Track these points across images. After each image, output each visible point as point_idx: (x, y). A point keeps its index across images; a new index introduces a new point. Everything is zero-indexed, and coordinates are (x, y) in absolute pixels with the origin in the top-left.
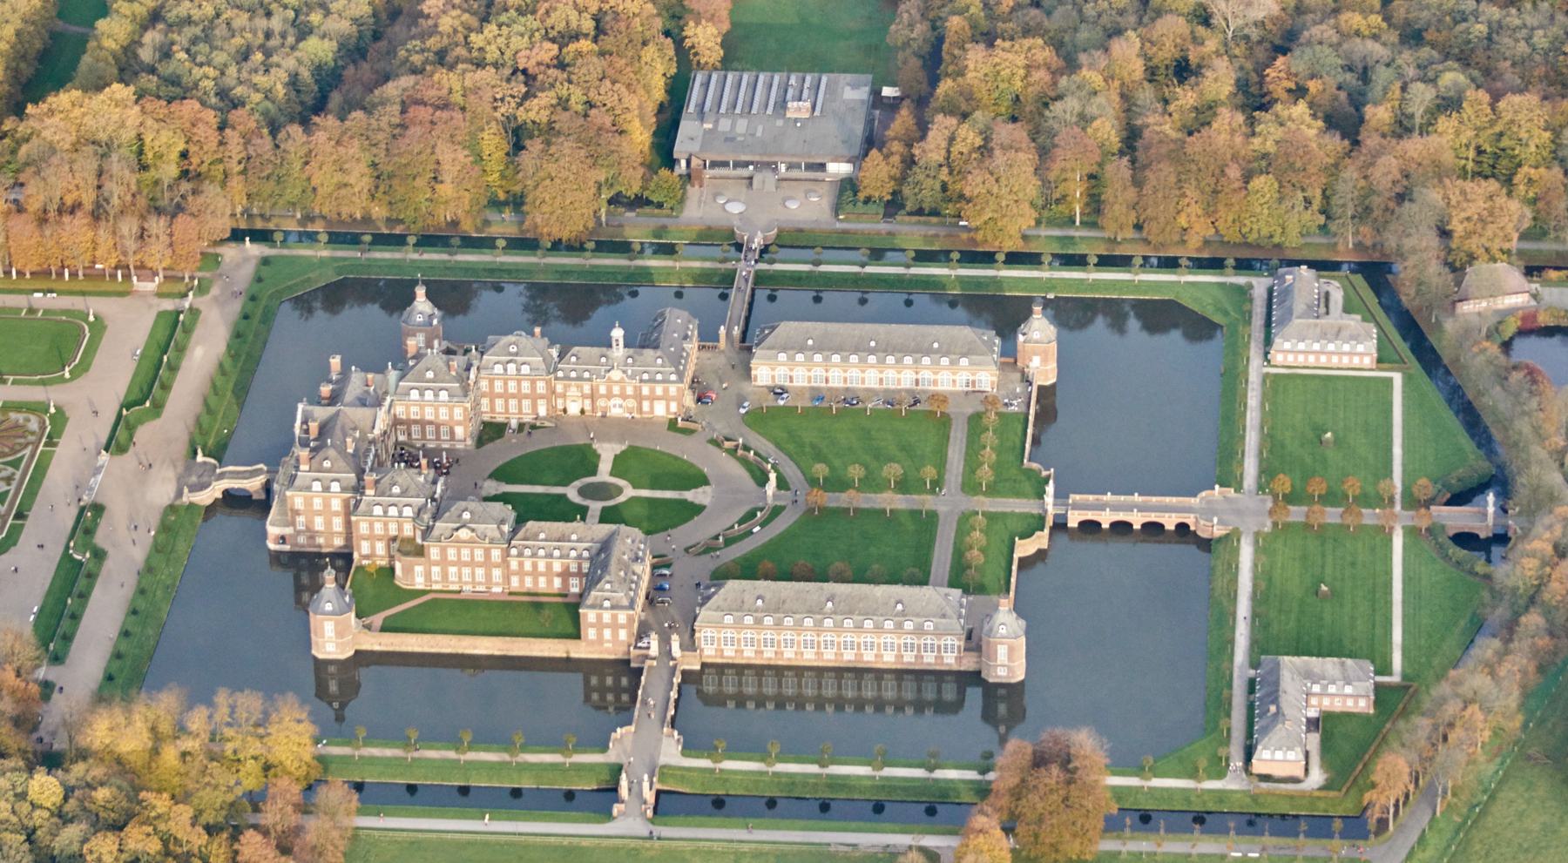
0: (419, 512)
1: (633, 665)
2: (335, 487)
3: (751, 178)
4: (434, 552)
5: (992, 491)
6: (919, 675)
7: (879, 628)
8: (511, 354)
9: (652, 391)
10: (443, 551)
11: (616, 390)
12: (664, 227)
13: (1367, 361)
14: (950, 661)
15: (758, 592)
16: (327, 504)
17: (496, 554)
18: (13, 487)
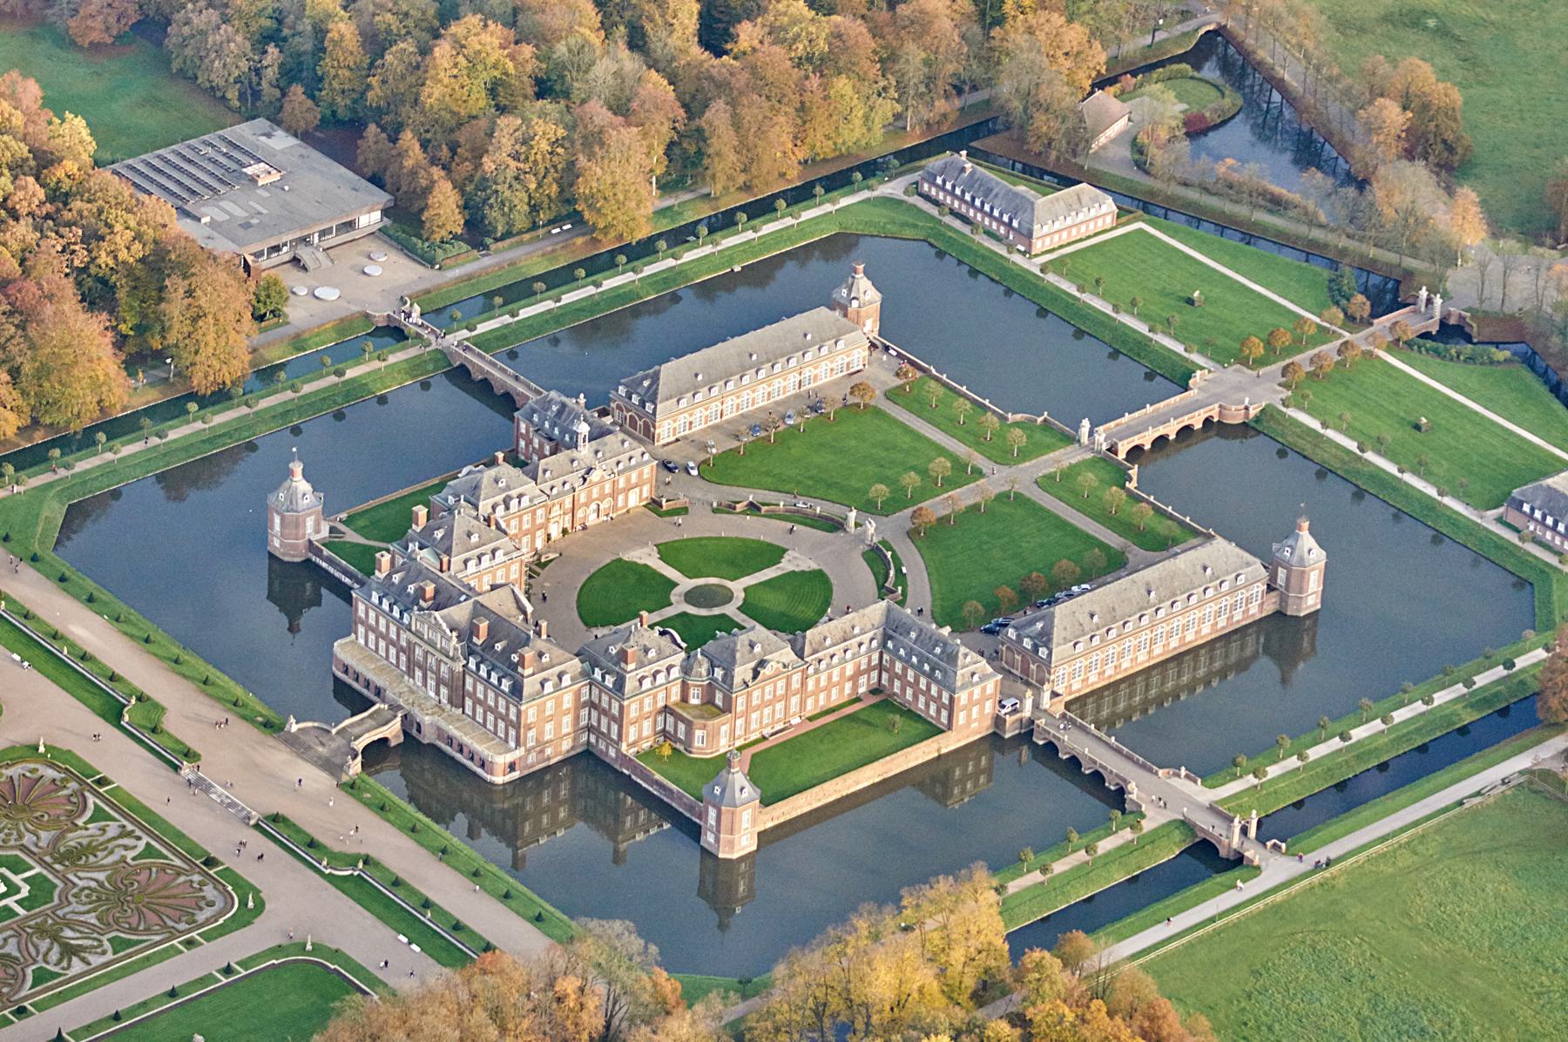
0: (686, 670)
1: (1007, 736)
2: (566, 680)
3: (295, 261)
4: (740, 703)
5: (1024, 455)
6: (1226, 638)
7: (1201, 603)
8: (503, 490)
9: (628, 480)
10: (749, 695)
11: (595, 492)
12: (297, 336)
13: (1109, 219)
14: (1255, 612)
15: (1087, 609)
16: (559, 704)
17: (796, 678)
18: (146, 839)
